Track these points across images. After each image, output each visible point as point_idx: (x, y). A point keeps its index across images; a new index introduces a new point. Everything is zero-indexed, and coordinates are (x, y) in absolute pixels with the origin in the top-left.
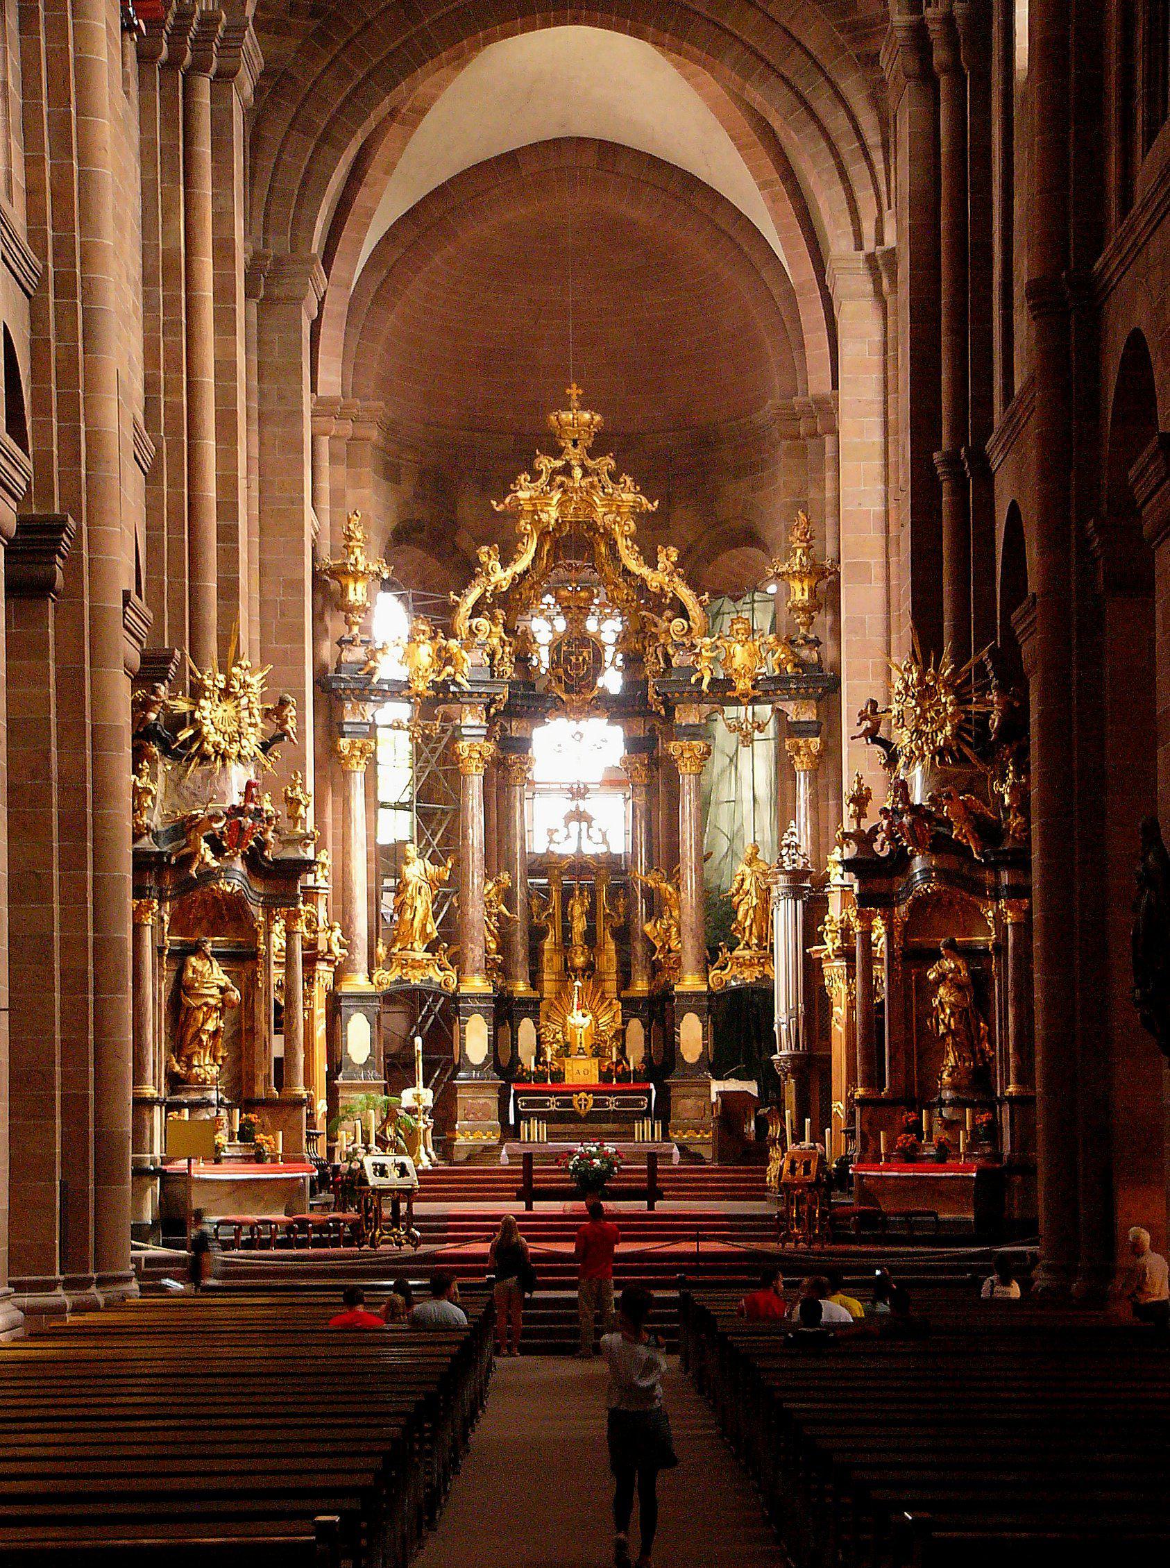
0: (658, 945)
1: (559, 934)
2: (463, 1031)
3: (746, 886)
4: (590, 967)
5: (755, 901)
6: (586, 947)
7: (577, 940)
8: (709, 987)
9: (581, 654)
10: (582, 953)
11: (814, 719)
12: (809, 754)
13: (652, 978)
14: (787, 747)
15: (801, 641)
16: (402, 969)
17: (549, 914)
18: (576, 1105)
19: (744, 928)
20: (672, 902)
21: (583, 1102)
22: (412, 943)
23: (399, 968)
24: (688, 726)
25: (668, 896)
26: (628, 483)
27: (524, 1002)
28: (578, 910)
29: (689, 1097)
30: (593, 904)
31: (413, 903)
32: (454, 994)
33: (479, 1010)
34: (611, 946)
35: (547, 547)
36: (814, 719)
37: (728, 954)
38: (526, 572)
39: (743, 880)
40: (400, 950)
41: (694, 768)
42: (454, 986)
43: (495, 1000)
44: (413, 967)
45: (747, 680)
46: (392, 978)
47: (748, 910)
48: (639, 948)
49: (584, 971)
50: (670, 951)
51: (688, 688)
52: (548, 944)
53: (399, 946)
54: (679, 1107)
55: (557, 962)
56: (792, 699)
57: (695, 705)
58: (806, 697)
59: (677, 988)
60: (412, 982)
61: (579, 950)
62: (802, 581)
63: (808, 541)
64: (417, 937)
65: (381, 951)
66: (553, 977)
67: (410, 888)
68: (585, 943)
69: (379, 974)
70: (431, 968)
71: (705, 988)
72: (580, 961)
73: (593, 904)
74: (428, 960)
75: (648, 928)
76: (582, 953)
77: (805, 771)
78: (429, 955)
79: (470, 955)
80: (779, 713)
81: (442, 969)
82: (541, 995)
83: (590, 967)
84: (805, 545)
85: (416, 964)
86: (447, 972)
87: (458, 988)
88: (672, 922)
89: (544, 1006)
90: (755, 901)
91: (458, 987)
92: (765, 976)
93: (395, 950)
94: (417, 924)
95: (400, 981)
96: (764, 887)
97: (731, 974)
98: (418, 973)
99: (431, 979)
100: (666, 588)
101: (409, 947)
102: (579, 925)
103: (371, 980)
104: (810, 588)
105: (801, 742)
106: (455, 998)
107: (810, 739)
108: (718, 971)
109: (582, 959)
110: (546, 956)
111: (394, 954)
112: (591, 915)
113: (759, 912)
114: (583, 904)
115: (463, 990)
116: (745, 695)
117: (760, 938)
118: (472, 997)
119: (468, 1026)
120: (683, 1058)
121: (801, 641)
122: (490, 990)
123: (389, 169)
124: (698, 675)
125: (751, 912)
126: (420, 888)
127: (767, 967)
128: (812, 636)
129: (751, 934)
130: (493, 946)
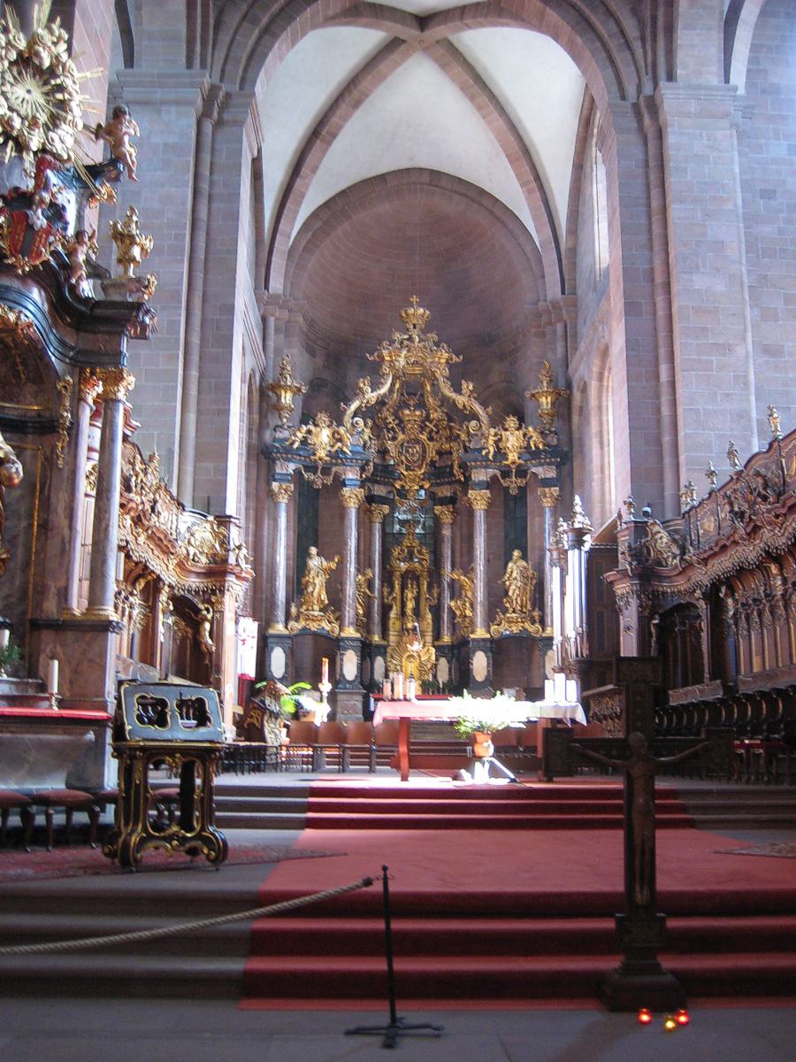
0: (458, 613)
1: (399, 609)
2: (342, 660)
3: (514, 575)
5: (519, 584)
7: (409, 612)
11: (555, 476)
13: (453, 633)
14: (539, 493)
27: (378, 647)
28: (410, 595)
33: (352, 648)
34: (429, 616)
37: (502, 616)
44: (313, 620)
46: (300, 627)
50: (465, 616)
52: (393, 614)
53: (304, 607)
57: (483, 470)
59: (472, 636)
65: (294, 610)
69: (292, 624)
71: (488, 636)
73: (418, 593)
78: (322, 614)
81: (330, 622)
89: (389, 650)
90: (519, 584)
93: (302, 610)
94: (315, 594)
95: (304, 629)
98: (315, 625)
102: (410, 605)
103: (286, 628)
105: (547, 490)
106: (338, 640)
110: (391, 621)
112: (417, 599)
115: (342, 635)
117: (521, 606)
118: (347, 639)
119: (345, 658)
122: (358, 635)
124: (487, 451)
128: (553, 429)
129: (517, 603)
130: (361, 612)
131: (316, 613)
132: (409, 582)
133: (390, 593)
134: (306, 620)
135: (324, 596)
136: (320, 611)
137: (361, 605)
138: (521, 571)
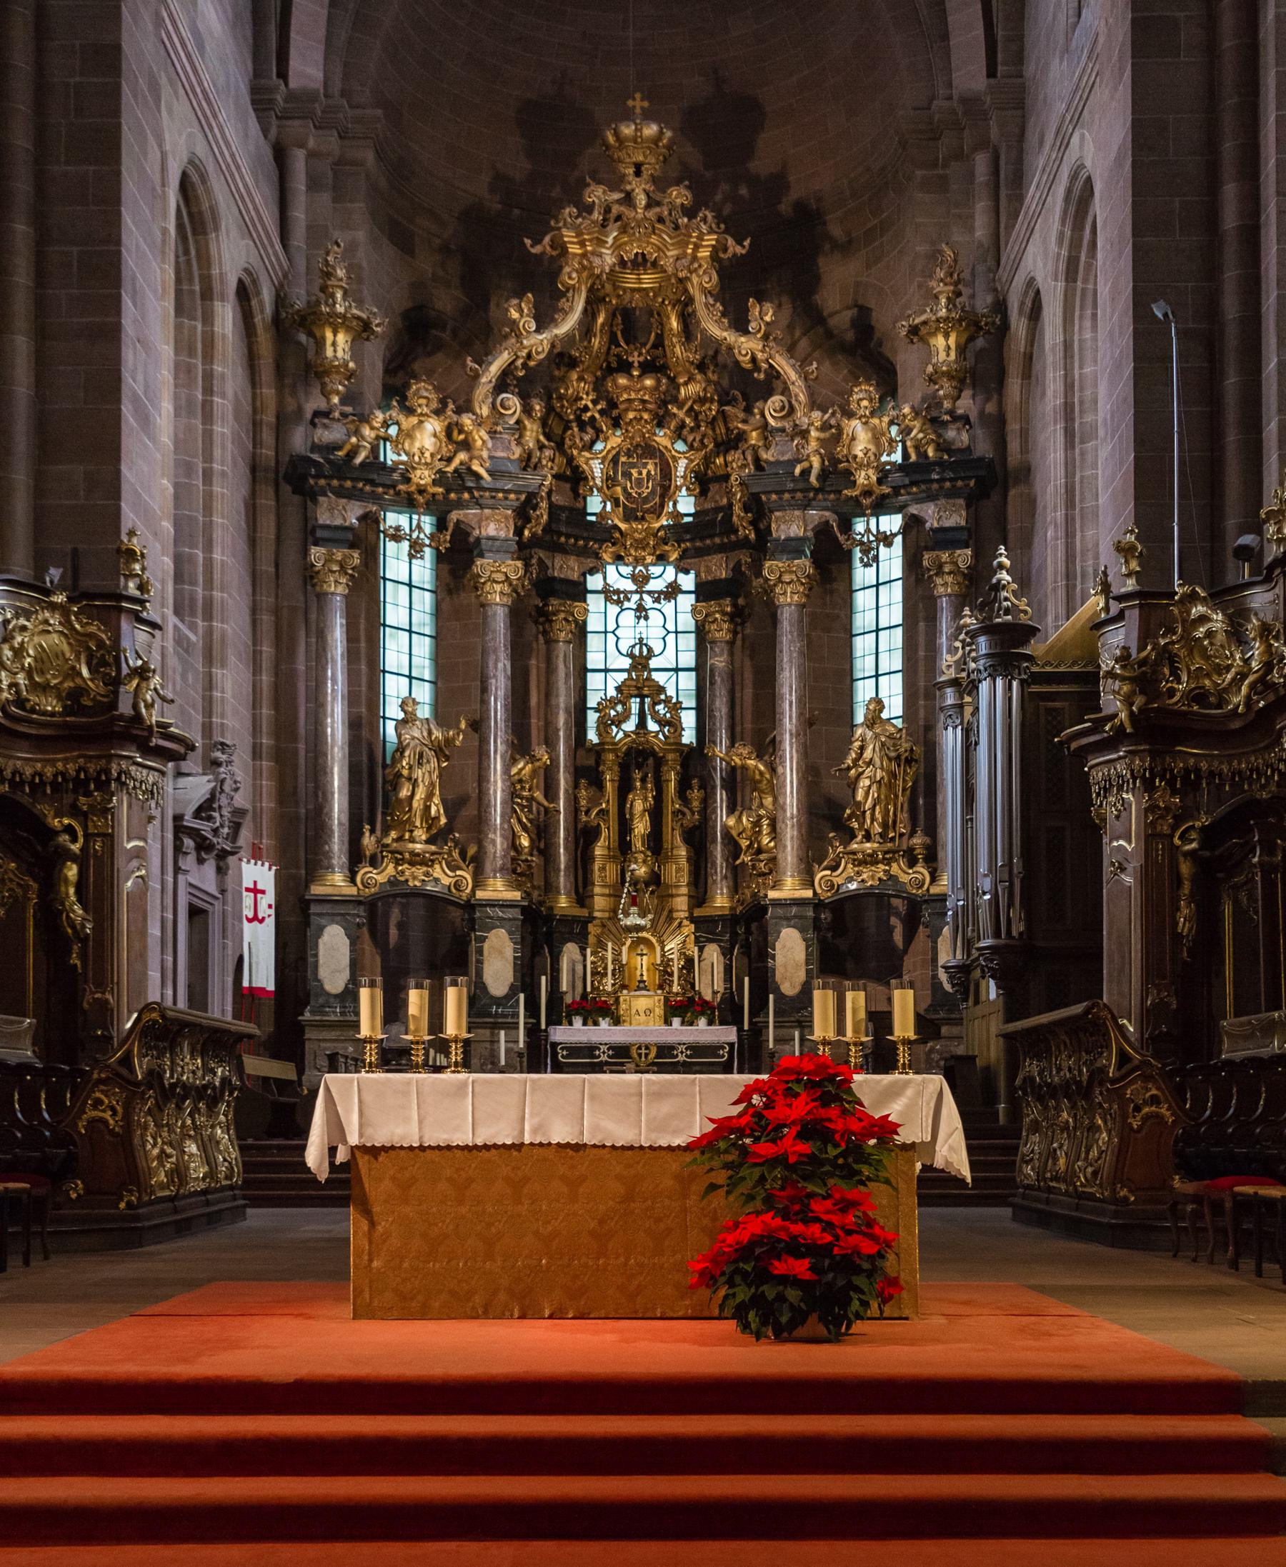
1: (615, 836)
2: (480, 951)
3: (868, 754)
4: (655, 879)
6: (649, 853)
7: (638, 844)
10: (644, 862)
11: (963, 523)
12: (956, 572)
13: (735, 889)
14: (925, 563)
16: (395, 868)
17: (602, 810)
20: (763, 785)
22: (411, 831)
23: (391, 866)
24: (789, 539)
25: (758, 777)
28: (639, 806)
30: (659, 799)
31: (410, 774)
32: (469, 901)
34: (683, 852)
36: (963, 523)
38: (569, 338)
41: (796, 597)
42: (468, 891)
43: (524, 910)
44: (412, 864)
46: (381, 878)
47: (870, 787)
48: (718, 852)
49: (647, 884)
51: (790, 486)
52: (599, 850)
53: (393, 834)
55: (612, 871)
56: (931, 497)
57: (797, 513)
58: (951, 494)
60: (411, 884)
61: (640, 857)
64: (418, 824)
65: (368, 841)
67: (407, 754)
68: (648, 849)
69: (364, 871)
70: (437, 866)
73: (659, 799)
74: (433, 854)
76: (644, 862)
77: (950, 595)
79: (490, 849)
80: (912, 526)
81: (453, 869)
83: (655, 879)
85: (416, 860)
86: (458, 873)
88: (762, 812)
91: (473, 891)
93: (388, 841)
95: (393, 882)
96: (893, 754)
98: (419, 871)
100: (759, 355)
101: (407, 835)
102: (641, 827)
104: (958, 346)
105: (945, 556)
106: (470, 906)
107: (958, 552)
109: (643, 870)
110: (597, 866)
111: (388, 845)
112: (656, 814)
113: (883, 789)
114: (645, 799)
115: (480, 894)
116: (867, 493)
118: (493, 904)
119: (486, 946)
122: (517, 895)
125: (874, 788)
128: (960, 412)
130: (525, 842)
131: (418, 847)
132: (637, 775)
133: (594, 801)
136: (428, 842)
137: (525, 828)
138: (883, 744)
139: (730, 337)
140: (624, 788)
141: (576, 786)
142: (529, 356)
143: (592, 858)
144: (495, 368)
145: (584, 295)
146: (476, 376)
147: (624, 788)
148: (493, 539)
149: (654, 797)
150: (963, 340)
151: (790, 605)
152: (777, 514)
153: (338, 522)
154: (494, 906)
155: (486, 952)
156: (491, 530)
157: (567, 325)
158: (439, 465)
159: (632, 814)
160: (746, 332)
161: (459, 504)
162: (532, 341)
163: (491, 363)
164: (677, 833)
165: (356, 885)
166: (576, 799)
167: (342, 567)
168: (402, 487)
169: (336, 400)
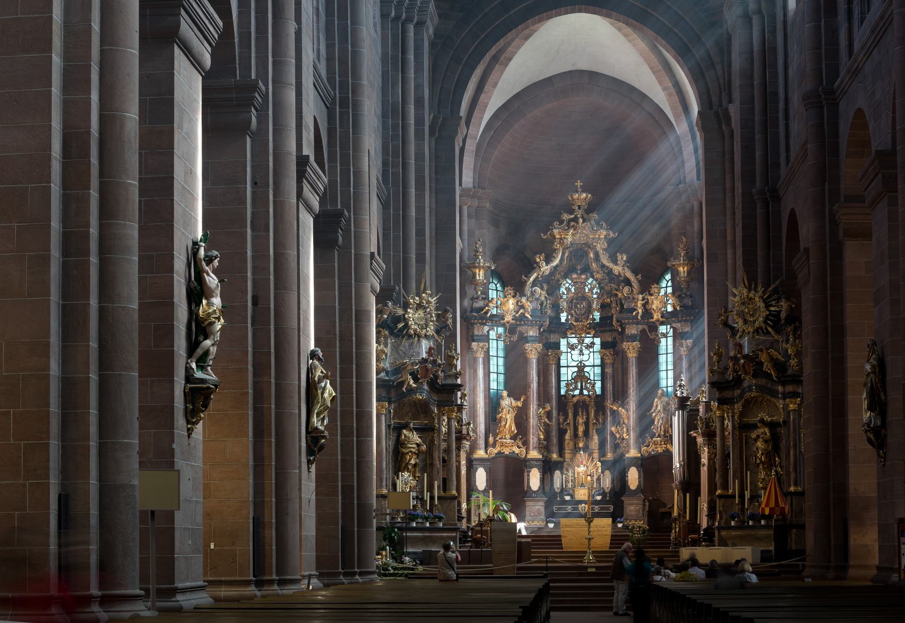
0: (618, 436)
2: (529, 476)
3: (659, 408)
7: (580, 433)
8: (642, 455)
9: (582, 303)
10: (583, 441)
15: (684, 296)
16: (501, 447)
18: (580, 510)
19: (658, 428)
21: (583, 508)
22: (505, 436)
26: (604, 225)
28: (581, 421)
29: (632, 504)
30: (588, 419)
32: (524, 459)
35: (566, 255)
37: (650, 440)
38: (557, 266)
39: (657, 406)
40: (500, 439)
43: (543, 462)
44: (506, 446)
45: (658, 314)
46: (496, 451)
50: (623, 439)
52: (567, 437)
53: (499, 436)
54: (628, 510)
55: (571, 444)
57: (634, 326)
58: (686, 321)
59: (627, 455)
60: (505, 453)
62: (684, 268)
63: (686, 250)
65: (491, 439)
66: (570, 452)
69: (490, 449)
71: (640, 455)
72: (581, 445)
73: (588, 419)
74: (513, 443)
75: (613, 429)
76: (583, 441)
78: (513, 441)
80: (675, 330)
81: (519, 447)
82: (564, 460)
84: (685, 252)
87: (526, 456)
92: (667, 449)
93: (498, 439)
95: (499, 453)
97: (651, 449)
99: (514, 452)
102: (581, 429)
103: (486, 453)
104: (687, 271)
108: (646, 448)
110: (567, 442)
111: (497, 441)
112: (587, 424)
114: (583, 419)
115: (528, 457)
117: (665, 432)
118: (533, 460)
119: (531, 474)
120: (629, 487)
121: (684, 296)
122: (541, 457)
123: (495, 85)
124: (637, 312)
126: (509, 410)
127: (668, 445)
130: (542, 437)
133: (565, 420)
134: (501, 446)
135: (513, 428)
139: (611, 265)
140: (575, 415)
141: (559, 415)
142: (543, 273)
143: (565, 440)
144: (532, 279)
145: (561, 252)
146: (526, 282)
147: (575, 415)
148: (532, 336)
149: (586, 418)
150: (690, 268)
151: (632, 357)
152: (628, 326)
153: (481, 333)
154: (533, 460)
155: (530, 476)
156: (531, 333)
157: (556, 262)
158: (514, 314)
159: (578, 424)
160: (616, 264)
161: (520, 325)
162: (544, 269)
163: (531, 277)
164: (594, 431)
165: (487, 454)
166: (559, 420)
167: (482, 349)
168: (502, 321)
169: (479, 293)
